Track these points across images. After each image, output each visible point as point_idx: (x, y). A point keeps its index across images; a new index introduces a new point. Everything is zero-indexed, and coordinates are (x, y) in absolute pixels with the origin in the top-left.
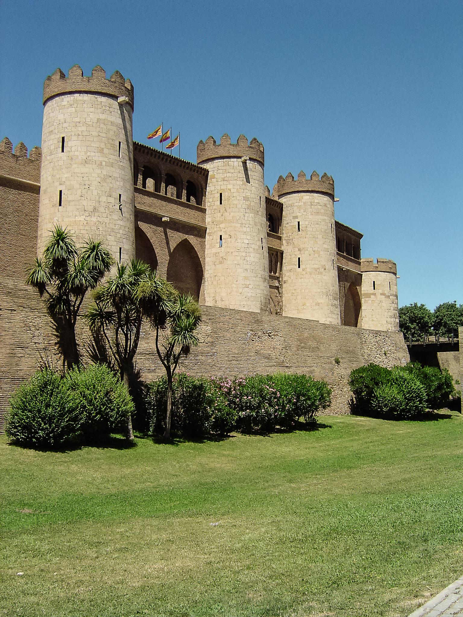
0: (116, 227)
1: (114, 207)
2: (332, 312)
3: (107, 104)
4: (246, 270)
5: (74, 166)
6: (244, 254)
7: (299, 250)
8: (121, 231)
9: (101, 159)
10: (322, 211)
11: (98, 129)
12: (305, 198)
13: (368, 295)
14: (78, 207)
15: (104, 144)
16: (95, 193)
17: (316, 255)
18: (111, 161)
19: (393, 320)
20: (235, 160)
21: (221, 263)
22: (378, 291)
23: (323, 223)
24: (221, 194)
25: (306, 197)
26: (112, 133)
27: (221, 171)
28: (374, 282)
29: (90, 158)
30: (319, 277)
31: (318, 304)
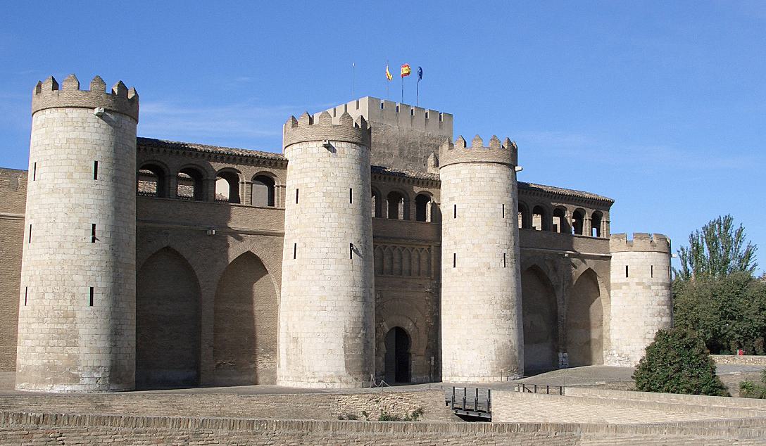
0: (87, 263)
1: (84, 241)
2: (497, 327)
3: (80, 120)
4: (324, 287)
5: (42, 196)
6: (321, 267)
7: (455, 243)
8: (93, 268)
9: (69, 185)
10: (487, 189)
11: (67, 151)
12: (463, 172)
13: (619, 286)
14: (43, 244)
15: (74, 168)
16: (61, 226)
17: (476, 250)
18: (82, 186)
19: (655, 319)
20: (315, 143)
21: (294, 279)
22: (634, 278)
23: (488, 205)
24: (298, 190)
25: (465, 170)
26: (84, 152)
27: (298, 161)
28: (627, 267)
29: (57, 186)
30: (480, 280)
31: (476, 316)
